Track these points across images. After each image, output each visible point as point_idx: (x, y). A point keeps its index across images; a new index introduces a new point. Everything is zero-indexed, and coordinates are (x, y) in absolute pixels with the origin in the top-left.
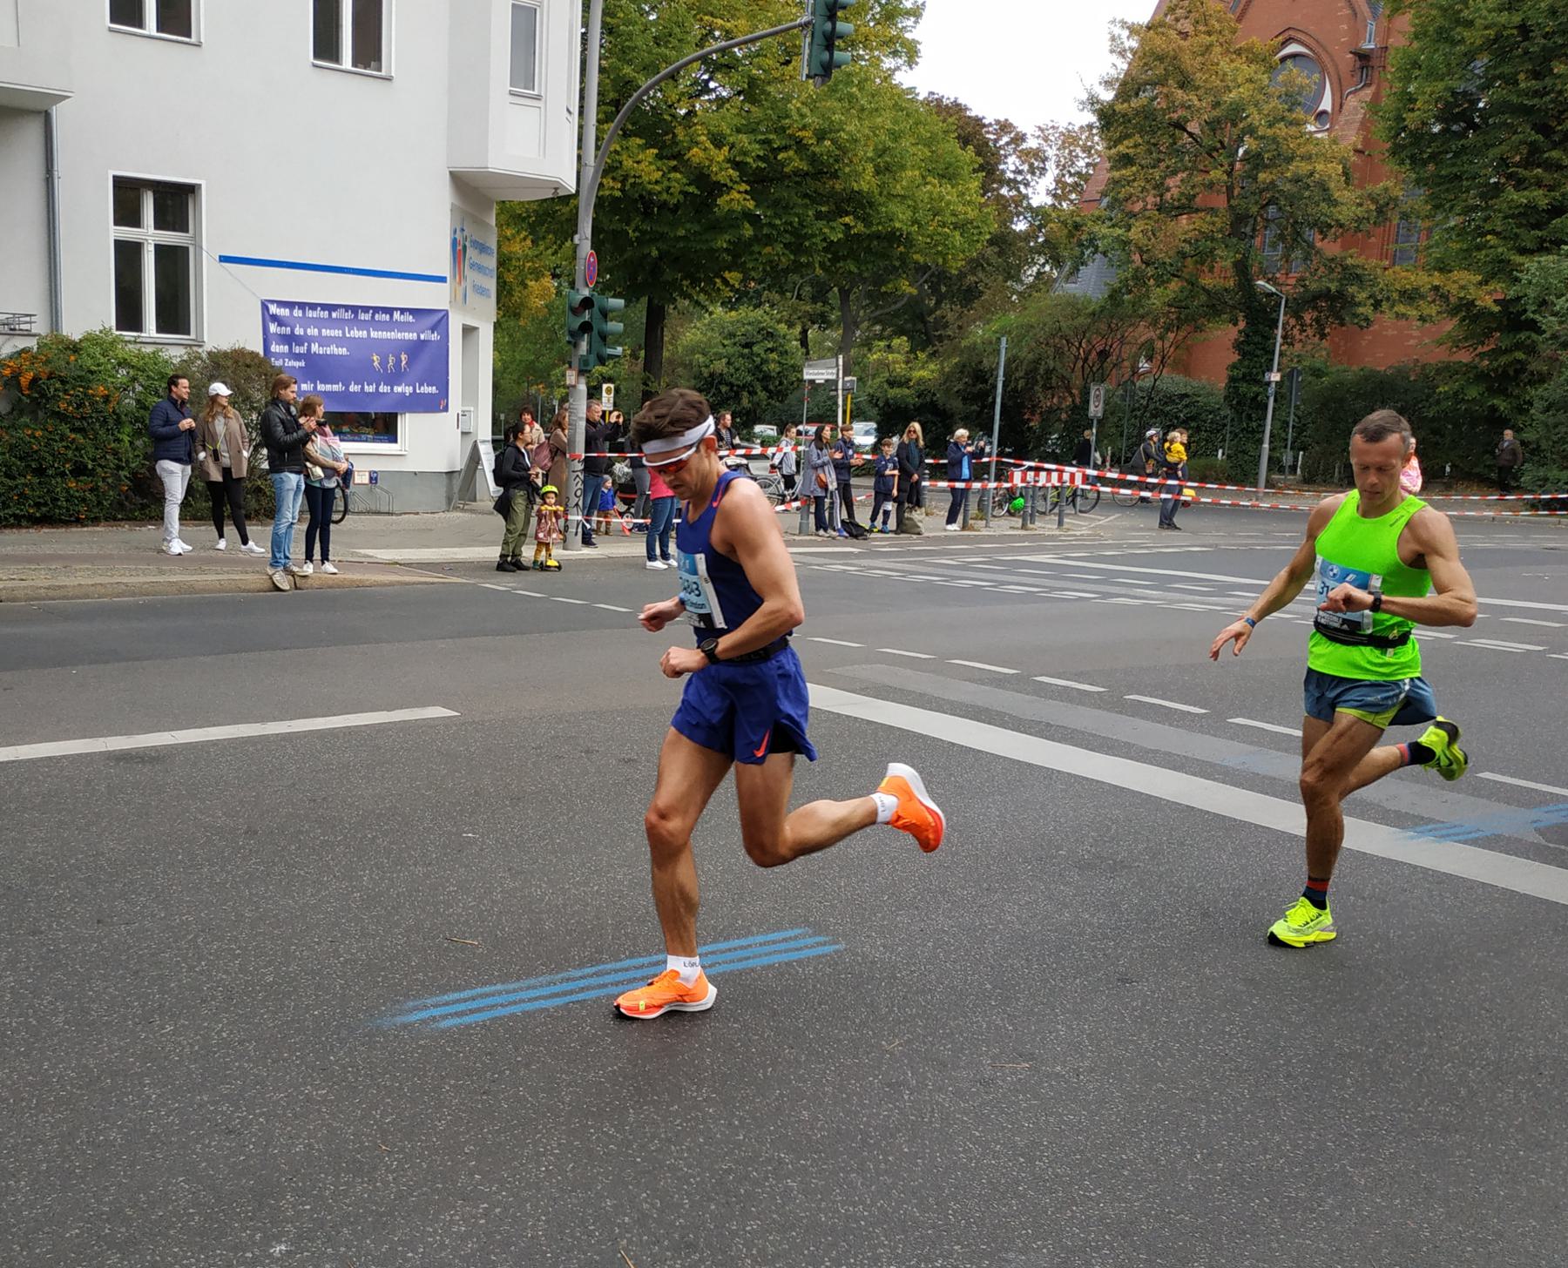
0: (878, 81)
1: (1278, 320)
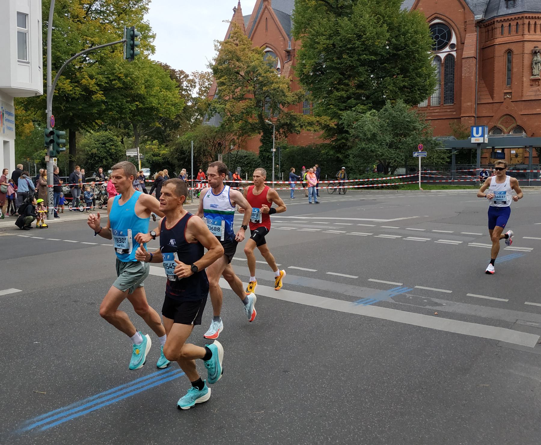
0: (143, 58)
1: (273, 132)
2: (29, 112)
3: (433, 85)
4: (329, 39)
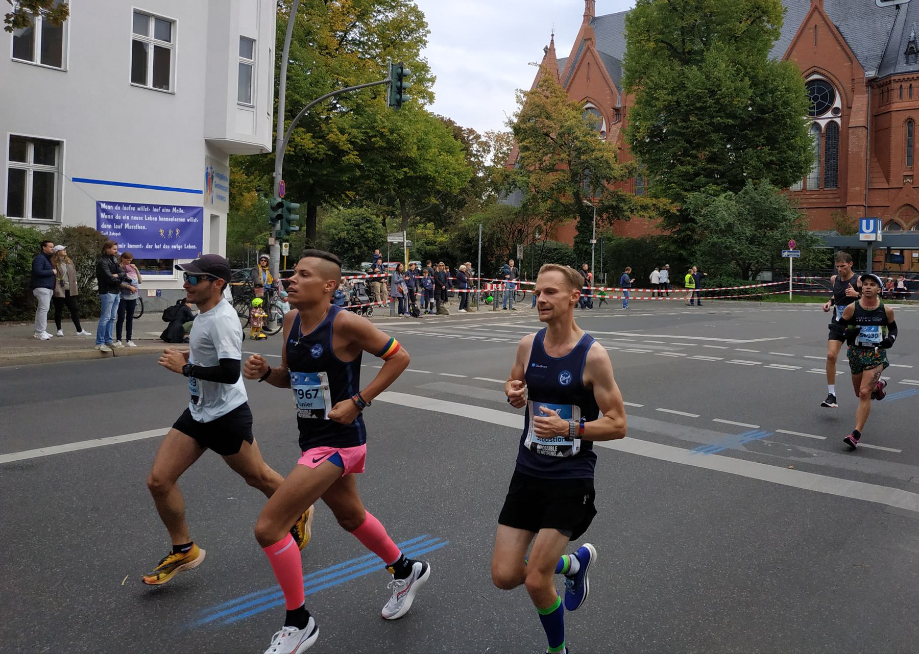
0: (416, 108)
1: (593, 217)
2: (252, 177)
3: (810, 161)
4: (672, 94)
